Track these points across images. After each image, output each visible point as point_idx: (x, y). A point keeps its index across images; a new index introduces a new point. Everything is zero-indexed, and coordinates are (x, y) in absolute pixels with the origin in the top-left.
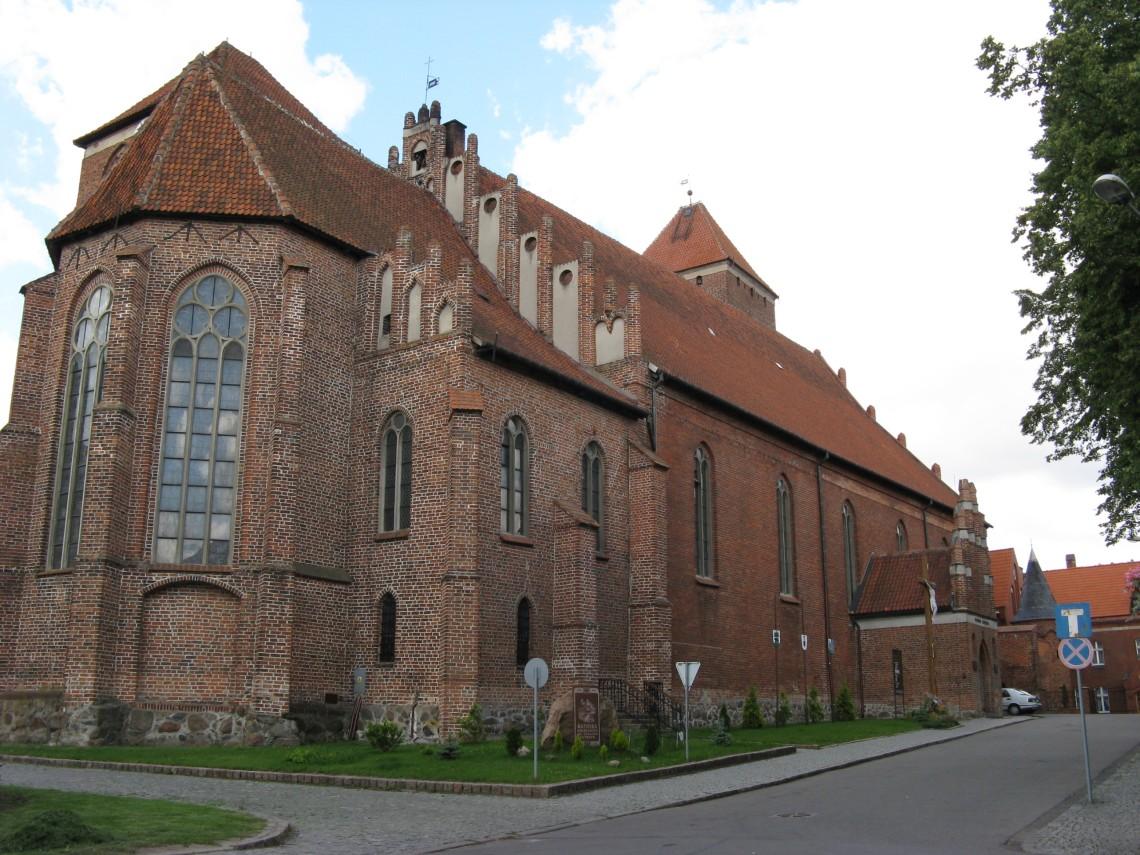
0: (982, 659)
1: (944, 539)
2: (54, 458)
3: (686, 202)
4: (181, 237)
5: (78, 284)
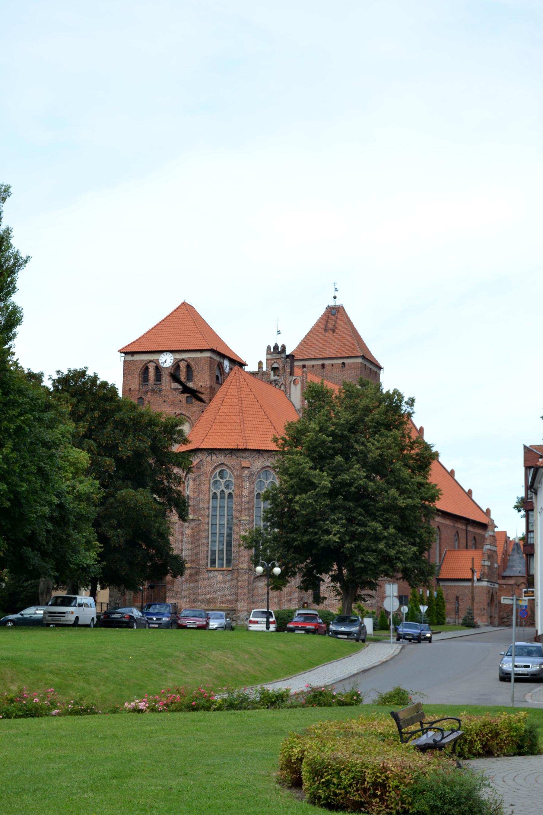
0: (491, 601)
1: (474, 537)
2: (208, 529)
3: (332, 304)
4: (257, 456)
5: (213, 467)
